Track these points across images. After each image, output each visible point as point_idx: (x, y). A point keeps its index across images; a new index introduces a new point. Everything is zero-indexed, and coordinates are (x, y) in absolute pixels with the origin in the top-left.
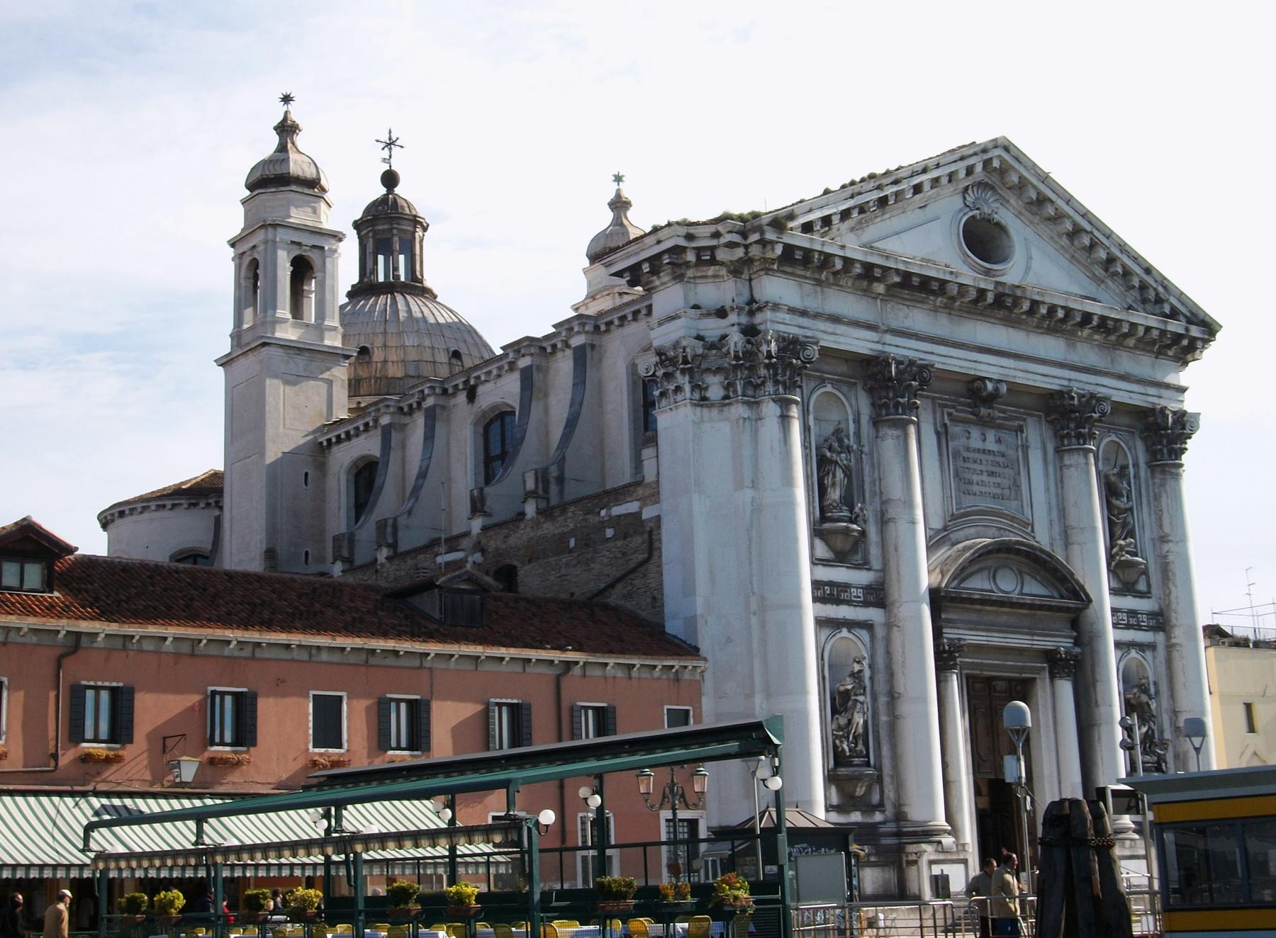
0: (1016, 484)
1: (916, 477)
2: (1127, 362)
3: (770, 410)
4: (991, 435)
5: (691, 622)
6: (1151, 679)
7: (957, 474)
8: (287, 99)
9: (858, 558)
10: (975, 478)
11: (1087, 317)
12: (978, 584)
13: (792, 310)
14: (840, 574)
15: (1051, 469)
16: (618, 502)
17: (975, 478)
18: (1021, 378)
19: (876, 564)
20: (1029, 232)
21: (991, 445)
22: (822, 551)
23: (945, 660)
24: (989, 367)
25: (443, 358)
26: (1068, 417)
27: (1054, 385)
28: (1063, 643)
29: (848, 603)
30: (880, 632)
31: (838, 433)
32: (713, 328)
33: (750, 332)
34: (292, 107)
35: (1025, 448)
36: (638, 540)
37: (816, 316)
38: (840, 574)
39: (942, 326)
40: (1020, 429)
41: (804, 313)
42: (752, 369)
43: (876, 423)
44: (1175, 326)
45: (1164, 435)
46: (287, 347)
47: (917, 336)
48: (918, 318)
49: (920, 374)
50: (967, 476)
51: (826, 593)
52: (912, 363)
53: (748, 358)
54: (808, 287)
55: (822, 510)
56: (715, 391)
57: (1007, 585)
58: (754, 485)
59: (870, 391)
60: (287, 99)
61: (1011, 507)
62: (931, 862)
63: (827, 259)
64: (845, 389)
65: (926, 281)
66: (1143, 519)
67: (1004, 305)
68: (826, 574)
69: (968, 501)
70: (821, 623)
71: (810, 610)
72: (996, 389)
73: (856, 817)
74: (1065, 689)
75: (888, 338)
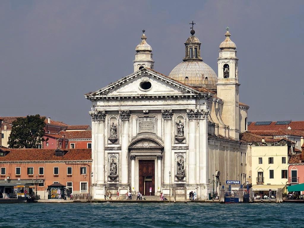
0: (154, 127)
4: (148, 119)
6: (184, 158)
7: (140, 126)
8: (144, 31)
10: (144, 127)
13: (101, 106)
15: (163, 123)
19: (120, 143)
23: (131, 158)
25: (183, 79)
28: (159, 153)
29: (114, 150)
30: (120, 154)
37: (106, 106)
39: (134, 103)
41: (103, 106)
47: (128, 106)
48: (130, 103)
50: (142, 127)
52: (124, 111)
57: (146, 145)
62: (120, 190)
63: (105, 98)
64: (117, 115)
65: (125, 98)
69: (142, 131)
72: (145, 112)
73: (113, 182)
75: (121, 107)
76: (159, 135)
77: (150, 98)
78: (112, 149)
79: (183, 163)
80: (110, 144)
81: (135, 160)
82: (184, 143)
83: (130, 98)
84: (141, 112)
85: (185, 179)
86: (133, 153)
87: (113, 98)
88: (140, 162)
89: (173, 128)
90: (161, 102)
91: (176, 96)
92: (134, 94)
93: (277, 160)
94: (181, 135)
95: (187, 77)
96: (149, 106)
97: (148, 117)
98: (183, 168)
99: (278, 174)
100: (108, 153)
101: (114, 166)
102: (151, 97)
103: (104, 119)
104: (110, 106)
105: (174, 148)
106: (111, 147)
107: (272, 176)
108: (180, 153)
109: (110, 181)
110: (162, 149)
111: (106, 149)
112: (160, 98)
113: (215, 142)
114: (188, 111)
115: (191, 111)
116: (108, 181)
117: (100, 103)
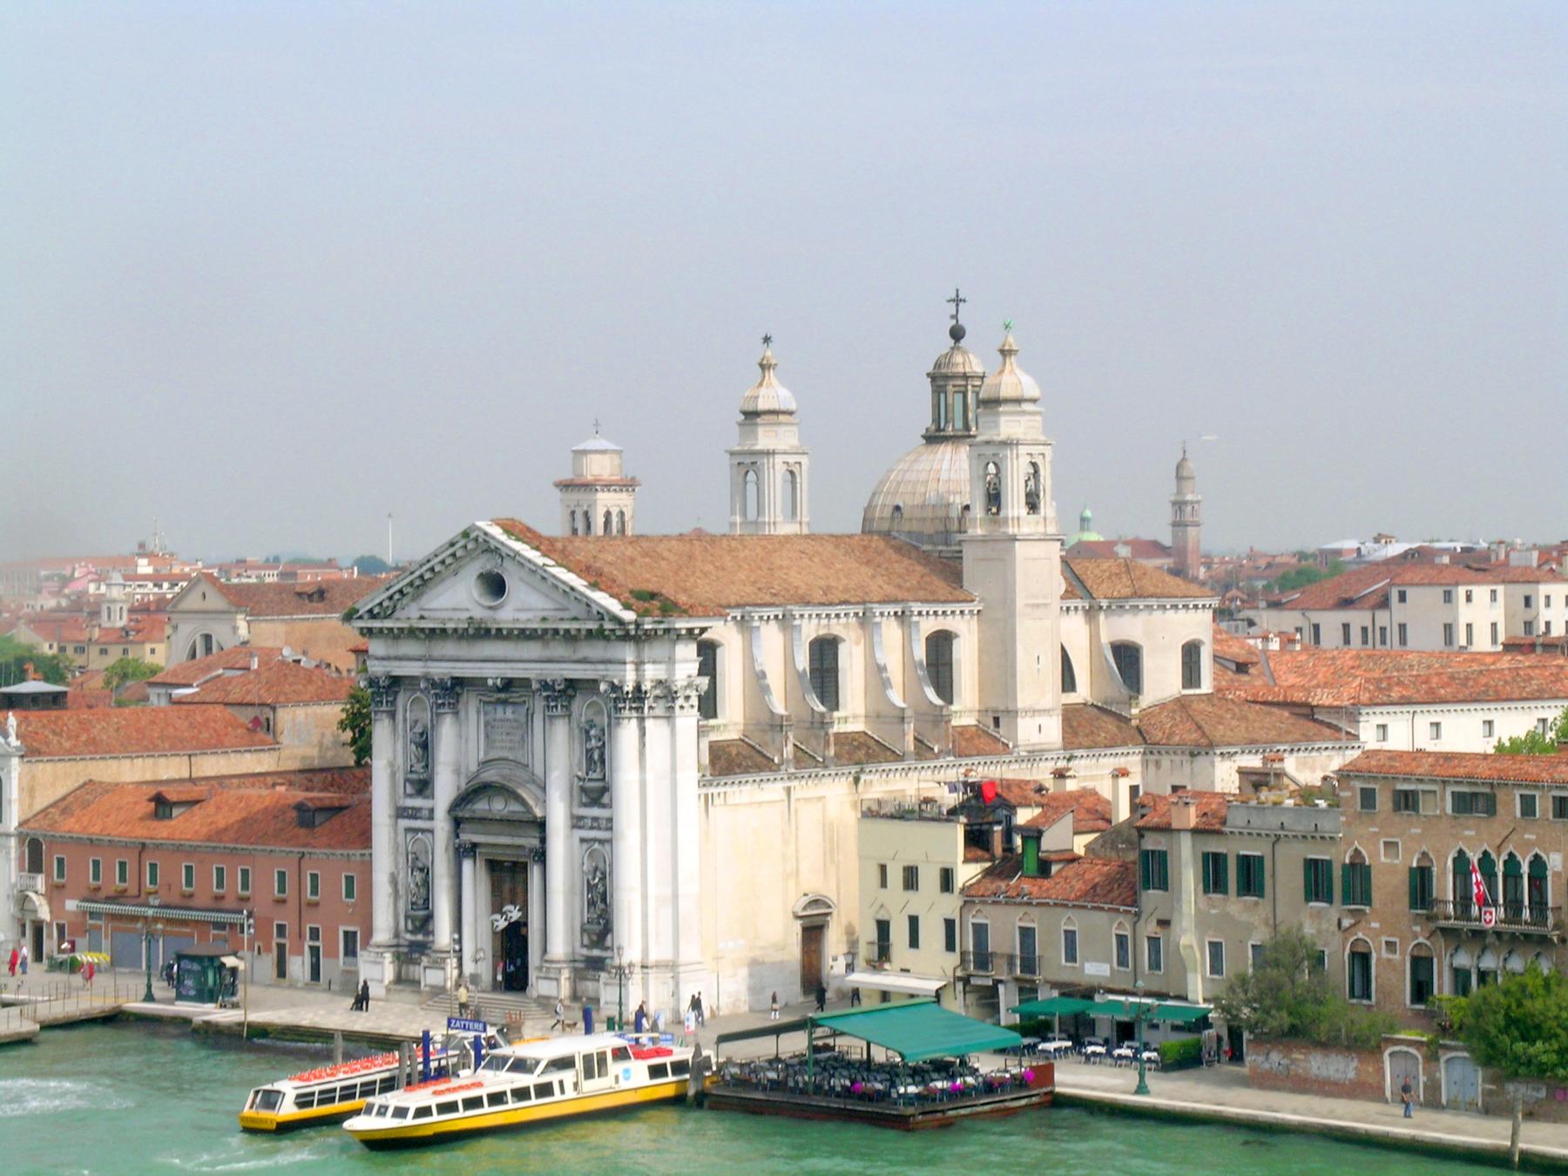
7: (487, 736)
8: (767, 340)
9: (428, 792)
10: (498, 738)
13: (377, 659)
17: (498, 738)
23: (462, 852)
25: (888, 512)
35: (529, 716)
48: (449, 648)
54: (390, 642)
57: (499, 806)
61: (519, 755)
63: (381, 630)
65: (433, 630)
69: (492, 755)
73: (420, 937)
75: (430, 664)
76: (539, 770)
77: (500, 635)
78: (414, 814)
79: (603, 879)
80: (410, 796)
81: (474, 857)
82: (604, 806)
83: (444, 630)
85: (608, 942)
86: (467, 837)
87: (401, 630)
88: (494, 866)
89: (577, 745)
90: (533, 649)
91: (567, 631)
92: (455, 621)
93: (929, 879)
94: (595, 776)
95: (897, 508)
96: (503, 665)
97: (505, 702)
98: (604, 900)
99: (933, 934)
100: (408, 830)
101: (419, 876)
102: (499, 630)
103: (393, 703)
105: (576, 822)
106: (412, 808)
107: (914, 942)
108: (594, 840)
109: (412, 932)
110: (541, 825)
111: (401, 813)
112: (525, 635)
113: (788, 790)
114: (603, 687)
115: (614, 688)
116: (407, 931)
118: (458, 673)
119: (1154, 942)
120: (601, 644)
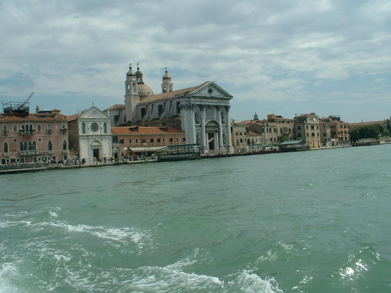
1: (204, 114)
2: (224, 101)
3: (192, 111)
4: (211, 110)
5: (184, 130)
11: (220, 98)
12: (209, 125)
14: (197, 125)
16: (177, 118)
18: (213, 105)
19: (200, 123)
20: (214, 89)
21: (210, 111)
22: (196, 123)
24: (210, 104)
25: (147, 93)
26: (218, 108)
27: (217, 105)
31: (197, 112)
32: (186, 103)
33: (190, 103)
34: (131, 65)
35: (214, 111)
36: (179, 122)
38: (197, 125)
40: (213, 109)
42: (190, 107)
43: (200, 110)
44: (228, 98)
45: (227, 108)
46: (133, 95)
48: (204, 100)
49: (204, 105)
51: (196, 126)
53: (189, 106)
55: (196, 119)
56: (186, 109)
58: (190, 117)
59: (200, 107)
60: (130, 64)
65: (205, 97)
66: (225, 117)
67: (212, 98)
68: (196, 125)
70: (196, 129)
71: (195, 128)
74: (217, 134)
76: (215, 119)
82: (224, 124)
84: (209, 106)
90: (216, 101)
95: (149, 92)
104: (197, 101)
117: (192, 99)
118: (206, 104)
119: (264, 138)
120: (226, 101)
